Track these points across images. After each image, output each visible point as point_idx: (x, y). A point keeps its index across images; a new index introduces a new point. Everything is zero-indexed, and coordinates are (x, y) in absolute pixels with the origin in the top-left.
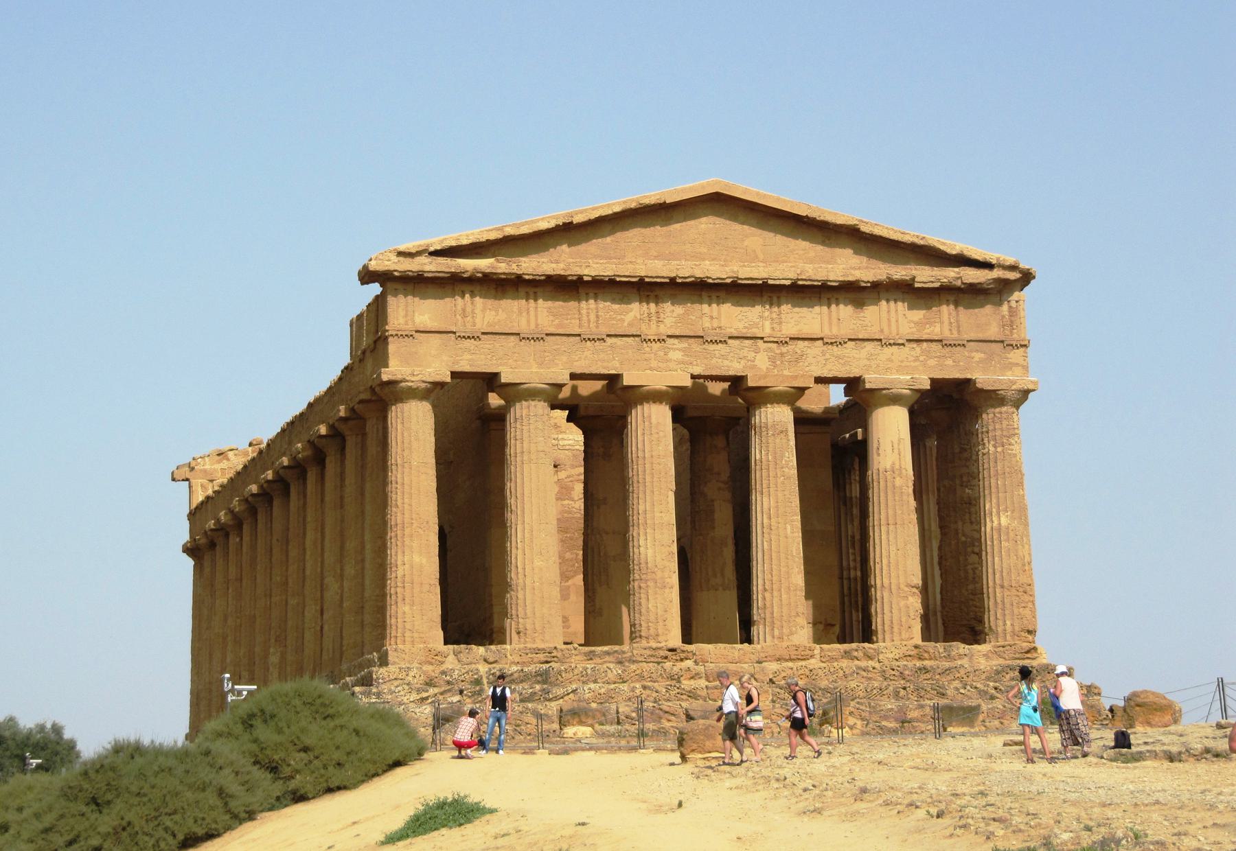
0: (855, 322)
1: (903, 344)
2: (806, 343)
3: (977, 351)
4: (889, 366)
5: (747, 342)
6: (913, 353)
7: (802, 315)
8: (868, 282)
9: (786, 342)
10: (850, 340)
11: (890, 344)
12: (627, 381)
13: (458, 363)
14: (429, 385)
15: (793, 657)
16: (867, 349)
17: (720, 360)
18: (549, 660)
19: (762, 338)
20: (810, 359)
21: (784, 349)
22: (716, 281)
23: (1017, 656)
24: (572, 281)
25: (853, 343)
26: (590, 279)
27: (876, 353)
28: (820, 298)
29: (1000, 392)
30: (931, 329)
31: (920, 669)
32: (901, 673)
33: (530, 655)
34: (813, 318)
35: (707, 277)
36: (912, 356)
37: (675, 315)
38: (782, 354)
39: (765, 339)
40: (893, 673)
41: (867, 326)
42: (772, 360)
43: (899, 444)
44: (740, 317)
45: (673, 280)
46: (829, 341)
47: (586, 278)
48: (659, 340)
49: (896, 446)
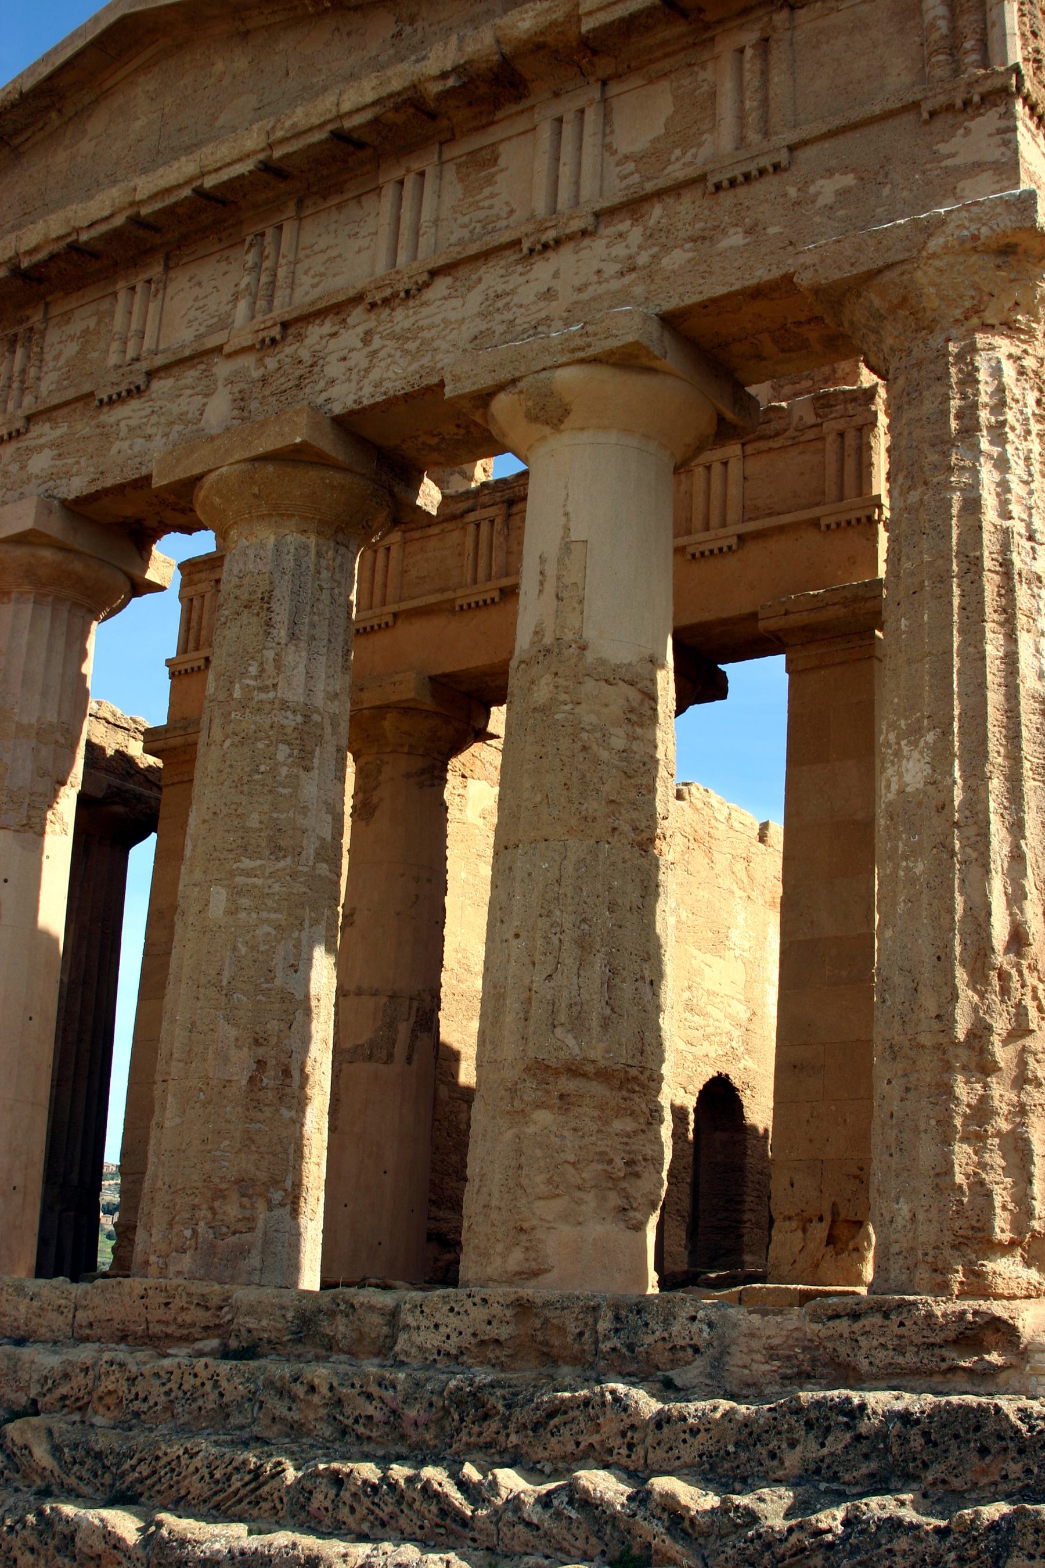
0: (466, 219)
1: (584, 233)
2: (327, 328)
3: (830, 172)
4: (543, 315)
5: (191, 375)
6: (620, 250)
7: (333, 253)
8: (444, 75)
9: (273, 341)
10: (434, 273)
11: (546, 247)
15: (156, 1329)
16: (482, 287)
19: (219, 349)
20: (334, 369)
21: (271, 363)
22: (94, 233)
23: (909, 1359)
25: (448, 280)
27: (509, 287)
28: (379, 189)
29: (889, 276)
30: (688, 157)
31: (459, 1400)
32: (394, 1412)
34: (359, 252)
36: (616, 259)
38: (264, 380)
39: (227, 349)
40: (370, 1409)
41: (498, 218)
42: (241, 401)
43: (560, 561)
44: (192, 314)
46: (378, 297)
48: (10, 434)
49: (551, 570)
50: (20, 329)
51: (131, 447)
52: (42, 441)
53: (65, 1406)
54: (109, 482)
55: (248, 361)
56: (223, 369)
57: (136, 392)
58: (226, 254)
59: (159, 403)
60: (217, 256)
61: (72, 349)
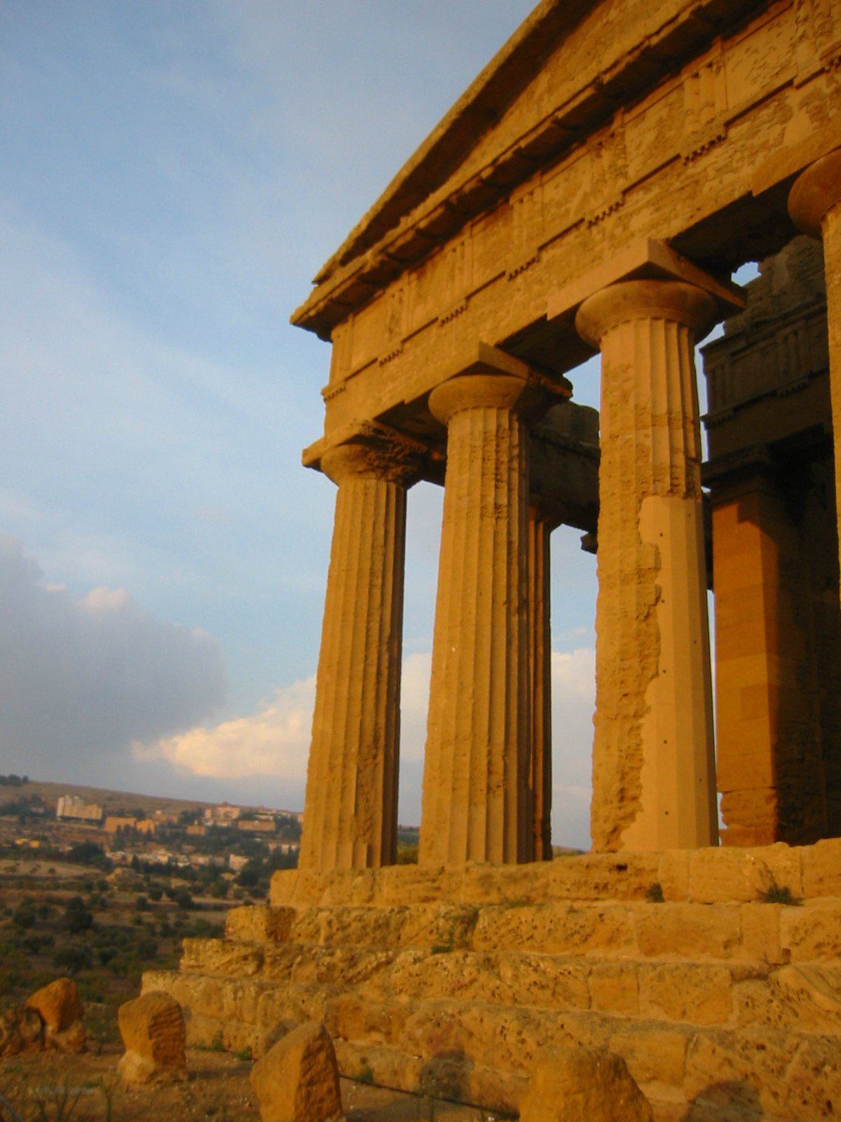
5: (765, 114)
12: (553, 311)
13: (380, 400)
14: (345, 448)
17: (715, 183)
18: (431, 894)
19: (789, 84)
22: (663, 34)
24: (472, 192)
26: (489, 172)
33: (409, 887)
35: (649, 37)
37: (643, 148)
39: (796, 82)
45: (596, 82)
47: (484, 175)
48: (611, 209)
50: (603, 139)
51: (721, 182)
52: (640, 204)
53: (820, 954)
54: (706, 212)
55: (821, 82)
56: (793, 98)
57: (720, 140)
58: (776, 21)
59: (740, 143)
60: (768, 26)
61: (650, 137)
